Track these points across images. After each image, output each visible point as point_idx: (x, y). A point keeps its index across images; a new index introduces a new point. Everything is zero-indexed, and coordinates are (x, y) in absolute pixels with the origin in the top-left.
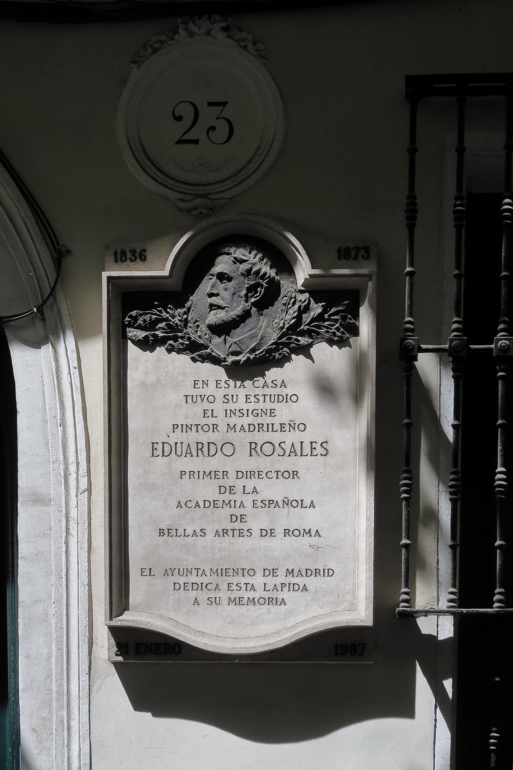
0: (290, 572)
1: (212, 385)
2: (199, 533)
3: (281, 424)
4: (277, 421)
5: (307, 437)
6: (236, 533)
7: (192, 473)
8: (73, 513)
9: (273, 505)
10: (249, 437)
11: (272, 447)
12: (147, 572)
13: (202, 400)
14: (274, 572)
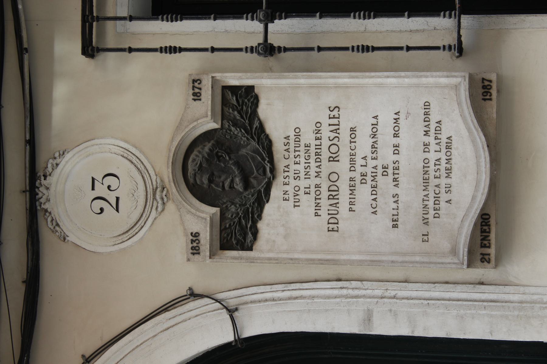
0: (426, 133)
1: (286, 188)
2: (396, 199)
3: (316, 139)
4: (313, 143)
5: (326, 121)
6: (396, 172)
7: (351, 203)
8: (378, 292)
9: (375, 145)
10: (325, 162)
11: (333, 146)
12: (426, 238)
13: (298, 195)
14: (426, 145)
